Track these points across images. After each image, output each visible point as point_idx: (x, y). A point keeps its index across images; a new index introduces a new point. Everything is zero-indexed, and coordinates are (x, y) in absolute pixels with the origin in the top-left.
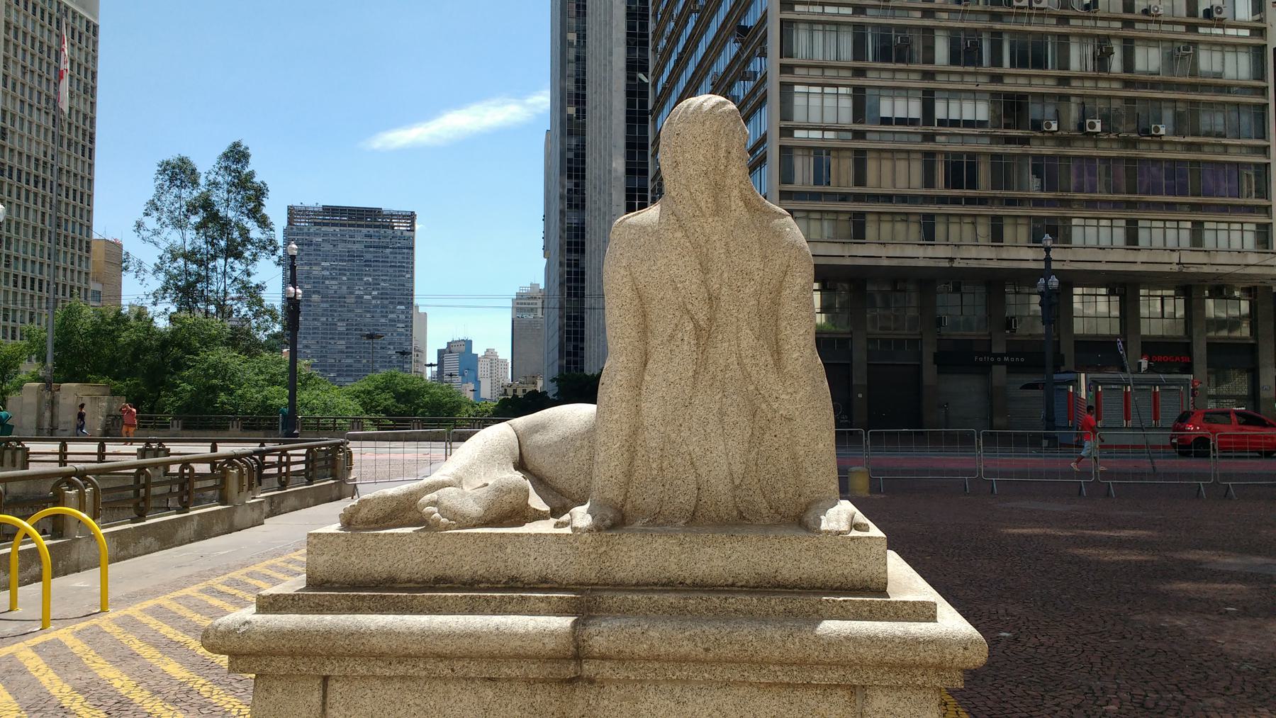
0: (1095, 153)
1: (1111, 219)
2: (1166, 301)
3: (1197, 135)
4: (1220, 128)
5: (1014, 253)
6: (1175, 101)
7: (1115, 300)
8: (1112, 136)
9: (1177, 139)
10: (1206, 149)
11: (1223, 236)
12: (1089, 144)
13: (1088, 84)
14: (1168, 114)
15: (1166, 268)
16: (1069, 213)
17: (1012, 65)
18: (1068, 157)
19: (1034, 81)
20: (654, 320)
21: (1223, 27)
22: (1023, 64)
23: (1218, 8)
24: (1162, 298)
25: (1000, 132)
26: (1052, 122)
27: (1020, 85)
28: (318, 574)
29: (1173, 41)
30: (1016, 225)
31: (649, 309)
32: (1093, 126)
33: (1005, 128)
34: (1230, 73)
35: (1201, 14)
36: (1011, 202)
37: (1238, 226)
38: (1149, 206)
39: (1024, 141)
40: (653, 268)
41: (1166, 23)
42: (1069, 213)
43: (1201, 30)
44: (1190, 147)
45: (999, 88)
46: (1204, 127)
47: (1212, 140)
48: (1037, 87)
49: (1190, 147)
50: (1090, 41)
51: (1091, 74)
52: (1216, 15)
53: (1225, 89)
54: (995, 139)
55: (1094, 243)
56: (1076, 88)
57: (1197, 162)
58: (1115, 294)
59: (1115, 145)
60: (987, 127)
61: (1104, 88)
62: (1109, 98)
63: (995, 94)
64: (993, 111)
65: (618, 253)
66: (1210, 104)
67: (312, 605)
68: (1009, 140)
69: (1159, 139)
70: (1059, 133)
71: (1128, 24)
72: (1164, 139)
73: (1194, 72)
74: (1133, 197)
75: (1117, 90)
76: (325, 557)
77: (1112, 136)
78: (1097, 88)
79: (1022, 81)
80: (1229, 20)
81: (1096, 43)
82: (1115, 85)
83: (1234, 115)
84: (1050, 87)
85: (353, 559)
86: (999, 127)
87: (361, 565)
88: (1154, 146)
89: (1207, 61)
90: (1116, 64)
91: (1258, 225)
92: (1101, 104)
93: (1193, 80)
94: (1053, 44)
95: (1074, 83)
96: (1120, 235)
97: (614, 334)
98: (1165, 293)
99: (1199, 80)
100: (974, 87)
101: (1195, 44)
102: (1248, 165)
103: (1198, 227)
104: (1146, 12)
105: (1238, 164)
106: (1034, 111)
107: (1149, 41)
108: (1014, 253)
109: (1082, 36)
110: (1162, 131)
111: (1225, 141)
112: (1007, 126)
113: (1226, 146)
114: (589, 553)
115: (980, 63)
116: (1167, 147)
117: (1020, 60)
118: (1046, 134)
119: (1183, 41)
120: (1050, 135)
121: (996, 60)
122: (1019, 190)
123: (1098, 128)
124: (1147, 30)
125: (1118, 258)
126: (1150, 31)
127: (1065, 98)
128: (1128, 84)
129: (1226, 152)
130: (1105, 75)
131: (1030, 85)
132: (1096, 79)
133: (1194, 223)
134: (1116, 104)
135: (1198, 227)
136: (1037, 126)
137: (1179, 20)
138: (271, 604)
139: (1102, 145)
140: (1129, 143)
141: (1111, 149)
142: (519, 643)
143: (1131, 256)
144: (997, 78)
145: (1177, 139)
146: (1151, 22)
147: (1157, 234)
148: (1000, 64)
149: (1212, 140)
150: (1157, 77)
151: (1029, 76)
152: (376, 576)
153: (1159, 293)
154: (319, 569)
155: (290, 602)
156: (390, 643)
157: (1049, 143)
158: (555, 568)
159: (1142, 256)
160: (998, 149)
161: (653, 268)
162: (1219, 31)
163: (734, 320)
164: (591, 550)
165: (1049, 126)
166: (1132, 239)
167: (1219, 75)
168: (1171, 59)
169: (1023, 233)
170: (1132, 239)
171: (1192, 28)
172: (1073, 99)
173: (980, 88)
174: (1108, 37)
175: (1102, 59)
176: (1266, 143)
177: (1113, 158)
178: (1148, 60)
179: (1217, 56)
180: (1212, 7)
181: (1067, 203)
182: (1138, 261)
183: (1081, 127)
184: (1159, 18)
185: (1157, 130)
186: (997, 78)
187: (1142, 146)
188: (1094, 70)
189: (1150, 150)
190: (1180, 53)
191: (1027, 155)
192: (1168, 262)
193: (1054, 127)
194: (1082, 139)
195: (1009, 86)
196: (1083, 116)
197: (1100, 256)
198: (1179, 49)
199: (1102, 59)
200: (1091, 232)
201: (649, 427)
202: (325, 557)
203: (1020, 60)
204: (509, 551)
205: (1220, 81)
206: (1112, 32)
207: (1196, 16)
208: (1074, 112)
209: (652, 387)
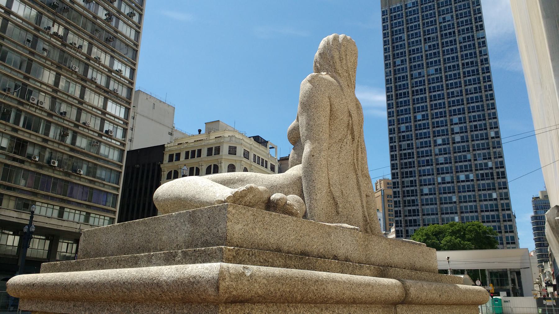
0: (52, 175)
1: (54, 205)
2: (69, 244)
3: (94, 177)
4: (103, 177)
5: (7, 213)
6: (89, 162)
7: (48, 242)
8: (61, 170)
9: (87, 177)
10: (97, 184)
11: (97, 220)
12: (50, 170)
13: (56, 145)
14: (85, 167)
15: (74, 230)
16: (35, 199)
17: (23, 126)
18: (40, 174)
19: (32, 137)
20: (333, 129)
21: (111, 139)
22: (29, 128)
23: (111, 131)
24: (68, 243)
25: (11, 155)
26: (36, 157)
27: (25, 136)
28: (235, 240)
29: (92, 138)
30: (9, 200)
31: (333, 123)
32: (54, 163)
33: (14, 153)
34: (111, 157)
35: (104, 131)
36: (9, 188)
37: (103, 217)
38: (69, 202)
39: (22, 162)
40: (341, 102)
41: (91, 130)
42: (35, 199)
43: (103, 137)
44: (91, 181)
45: (15, 134)
46: (98, 175)
47: (100, 181)
48: (33, 139)
49: (91, 181)
50: (60, 128)
51: (57, 141)
52: (109, 134)
53: (108, 162)
54: (8, 157)
55: (44, 214)
56: (49, 145)
57: (91, 188)
58: (48, 239)
59: (61, 174)
60: (5, 151)
61: (62, 149)
62: (63, 153)
63: (12, 137)
64: (10, 144)
65: (323, 89)
66: (102, 167)
67: (262, 261)
68: (14, 159)
69: (79, 175)
70: (39, 162)
71: (77, 126)
72: (82, 176)
73: (98, 152)
74: (65, 198)
75: (67, 151)
76: (240, 226)
77: (61, 170)
78: (59, 148)
79: (26, 135)
80: (114, 137)
81: (62, 129)
82: (66, 149)
83: (109, 173)
84: (38, 141)
85: (257, 230)
86: (11, 152)
87: (262, 236)
88: (77, 178)
89: (104, 150)
90: (68, 140)
91: (110, 218)
92: (59, 155)
93: (97, 155)
94: (44, 124)
95: (49, 143)
96: (56, 214)
97: (321, 130)
98: (69, 242)
99: (99, 156)
100: (3, 131)
101: (100, 142)
102: (111, 193)
103: (88, 215)
104: (84, 124)
105: (107, 192)
106: (30, 150)
107: (84, 136)
108: (7, 213)
109: (57, 125)
110: (82, 173)
111: (104, 182)
112: (15, 153)
113: (104, 184)
114: (362, 244)
115: (8, 121)
116: (82, 179)
117: (27, 125)
118: (33, 161)
119: (96, 140)
120: (35, 162)
121: (17, 122)
122: (14, 184)
123: (56, 165)
124: (83, 131)
125: (54, 223)
126: (84, 132)
127: (45, 148)
128: (72, 150)
129: (104, 187)
130: (63, 143)
131: (30, 138)
132: (59, 144)
133: (87, 213)
134: (65, 157)
135: (88, 215)
136: (29, 157)
137: (96, 131)
138: (234, 257)
139: (56, 172)
140: (67, 174)
141: (60, 175)
142: (387, 291)
143: (60, 223)
144: (16, 130)
145: (87, 177)
146: (85, 128)
147: (72, 215)
148: (18, 125)
149: (100, 181)
150: (83, 150)
151: (30, 134)
152: (270, 246)
153: (67, 241)
154: (236, 236)
155: (248, 256)
156: (337, 289)
157: (33, 165)
158: (350, 252)
159: (65, 224)
160: (8, 162)
161: (341, 102)
162: (110, 140)
163: (357, 142)
164: (362, 243)
165: (35, 158)
166: (61, 215)
167: (108, 156)
168: (91, 144)
169: (12, 204)
170: (61, 215)
171: (100, 135)
172: (48, 149)
173: (6, 132)
174: (68, 129)
175: (63, 136)
176: (119, 187)
177: (60, 179)
178: (81, 143)
179: (107, 149)
180: (109, 130)
181: (35, 194)
182: (63, 225)
183: (49, 162)
184: (89, 128)
185: (80, 171)
186: (16, 130)
187: (72, 177)
188: (59, 140)
189: (75, 179)
190: (95, 144)
191: (21, 168)
192: (73, 227)
193: (37, 159)
194: (48, 168)
195: (20, 135)
196: (50, 158)
197: (47, 220)
198: (94, 142)
199: (63, 136)
200: (44, 209)
201: (333, 185)
202: (240, 226)
203: (27, 125)
204: (332, 237)
205: (107, 159)
206: (70, 127)
207: (102, 132)
208: (47, 155)
209: (332, 164)
